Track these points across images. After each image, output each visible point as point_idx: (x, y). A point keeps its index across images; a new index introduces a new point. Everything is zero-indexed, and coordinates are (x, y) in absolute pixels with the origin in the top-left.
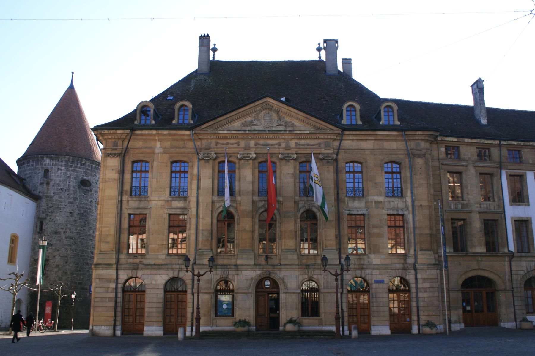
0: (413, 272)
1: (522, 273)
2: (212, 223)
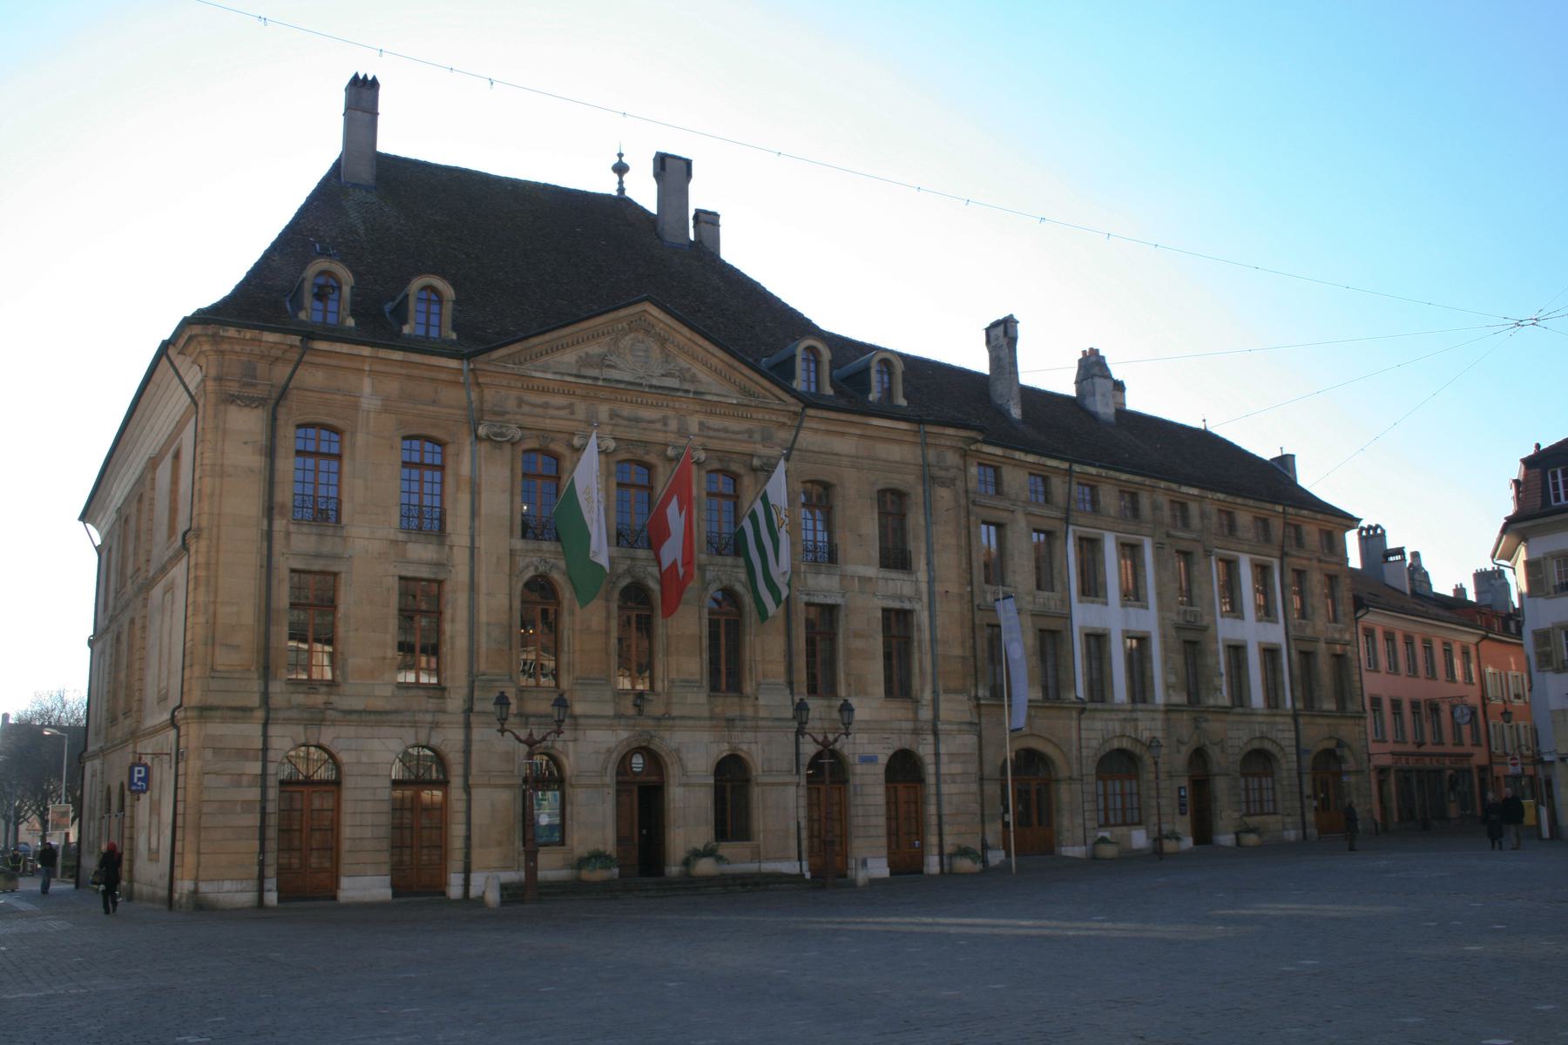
0: (930, 739)
1: (1094, 744)
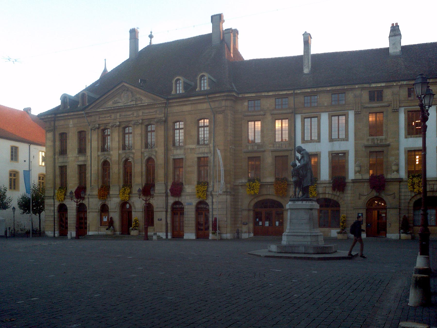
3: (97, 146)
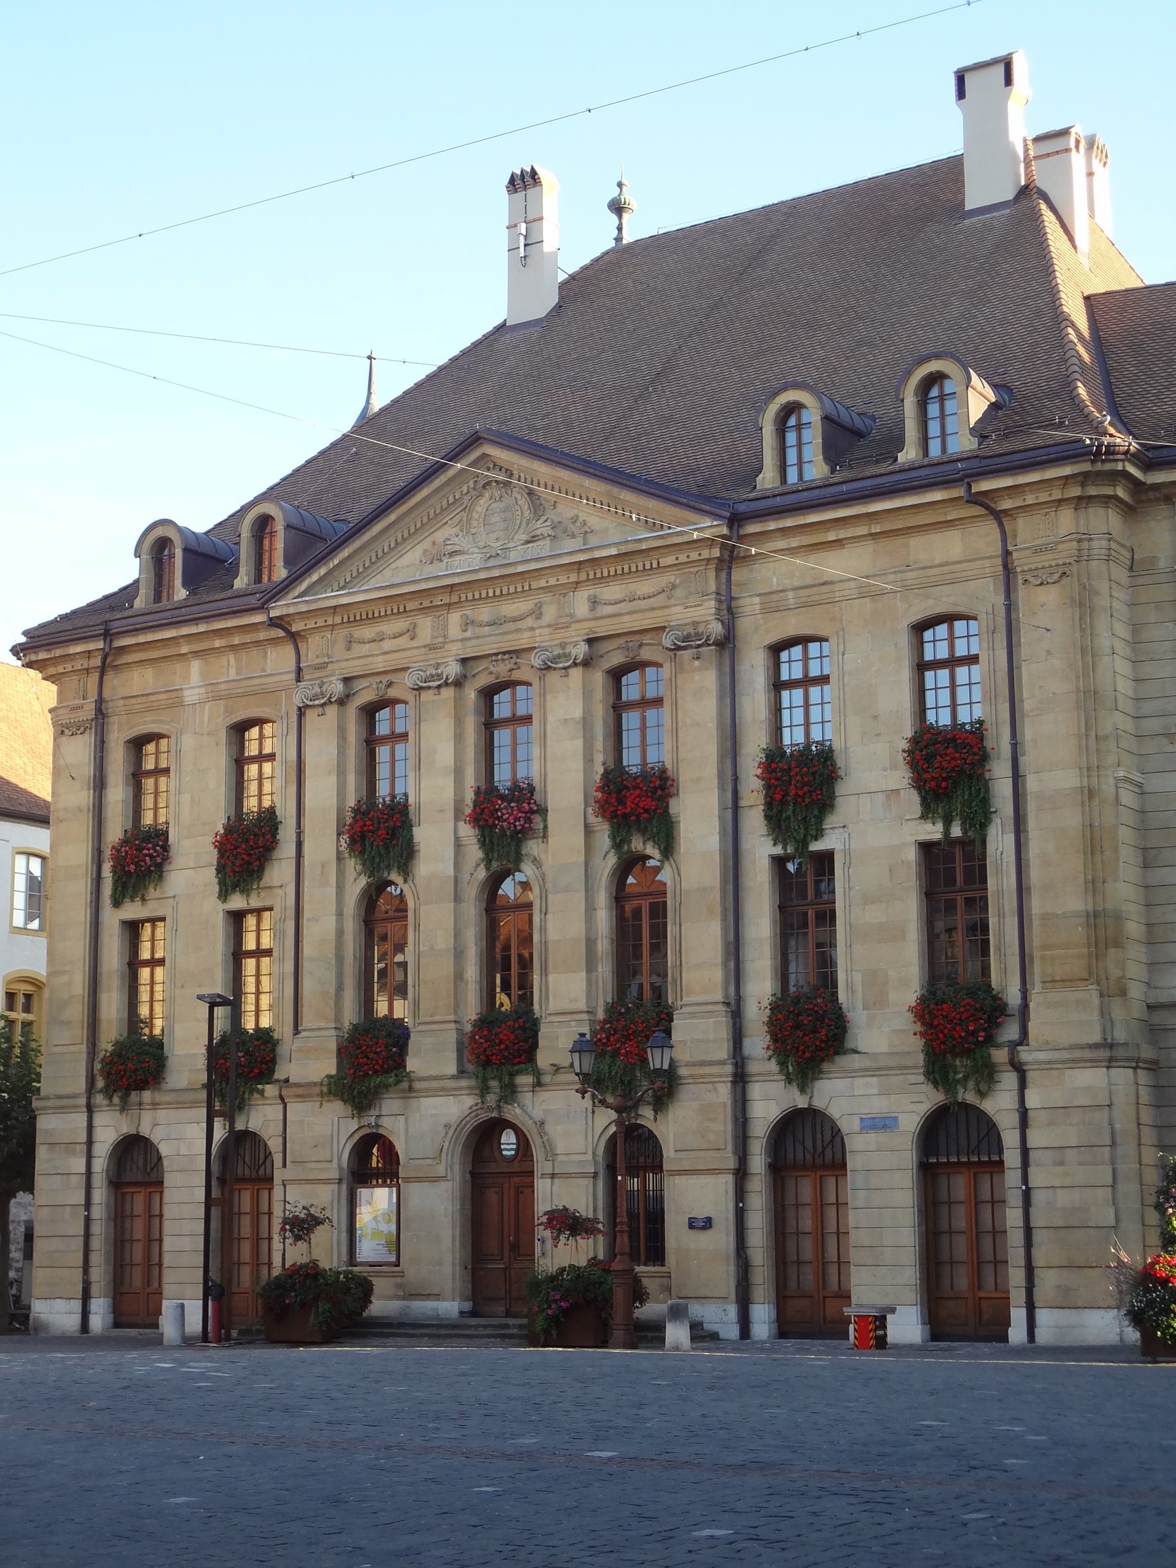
2: (340, 933)
3: (333, 801)
